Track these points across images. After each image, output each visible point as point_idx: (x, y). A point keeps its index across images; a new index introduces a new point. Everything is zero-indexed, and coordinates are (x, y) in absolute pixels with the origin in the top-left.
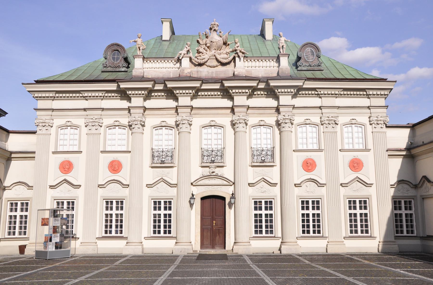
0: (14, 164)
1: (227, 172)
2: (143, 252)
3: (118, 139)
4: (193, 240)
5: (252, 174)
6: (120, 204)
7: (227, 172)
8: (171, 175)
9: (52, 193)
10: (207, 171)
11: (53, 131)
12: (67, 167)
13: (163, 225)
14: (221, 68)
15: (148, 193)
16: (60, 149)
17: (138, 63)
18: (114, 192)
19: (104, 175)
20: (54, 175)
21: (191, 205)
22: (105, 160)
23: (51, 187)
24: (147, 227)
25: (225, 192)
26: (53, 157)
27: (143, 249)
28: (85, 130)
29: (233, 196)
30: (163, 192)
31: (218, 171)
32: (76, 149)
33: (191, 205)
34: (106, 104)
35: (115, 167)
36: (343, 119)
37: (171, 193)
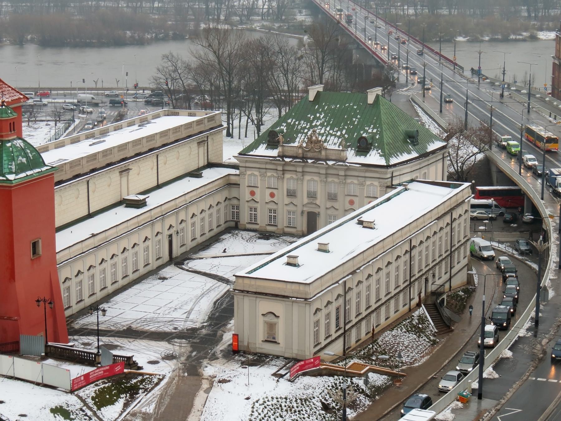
3: (273, 182)
6: (275, 211)
7: (318, 202)
8: (295, 201)
11: (246, 177)
12: (253, 193)
14: (315, 154)
19: (268, 199)
20: (248, 197)
21: (302, 215)
22: (268, 192)
23: (247, 201)
25: (316, 210)
28: (259, 178)
29: (319, 213)
33: (302, 215)
35: (272, 195)
36: (368, 183)
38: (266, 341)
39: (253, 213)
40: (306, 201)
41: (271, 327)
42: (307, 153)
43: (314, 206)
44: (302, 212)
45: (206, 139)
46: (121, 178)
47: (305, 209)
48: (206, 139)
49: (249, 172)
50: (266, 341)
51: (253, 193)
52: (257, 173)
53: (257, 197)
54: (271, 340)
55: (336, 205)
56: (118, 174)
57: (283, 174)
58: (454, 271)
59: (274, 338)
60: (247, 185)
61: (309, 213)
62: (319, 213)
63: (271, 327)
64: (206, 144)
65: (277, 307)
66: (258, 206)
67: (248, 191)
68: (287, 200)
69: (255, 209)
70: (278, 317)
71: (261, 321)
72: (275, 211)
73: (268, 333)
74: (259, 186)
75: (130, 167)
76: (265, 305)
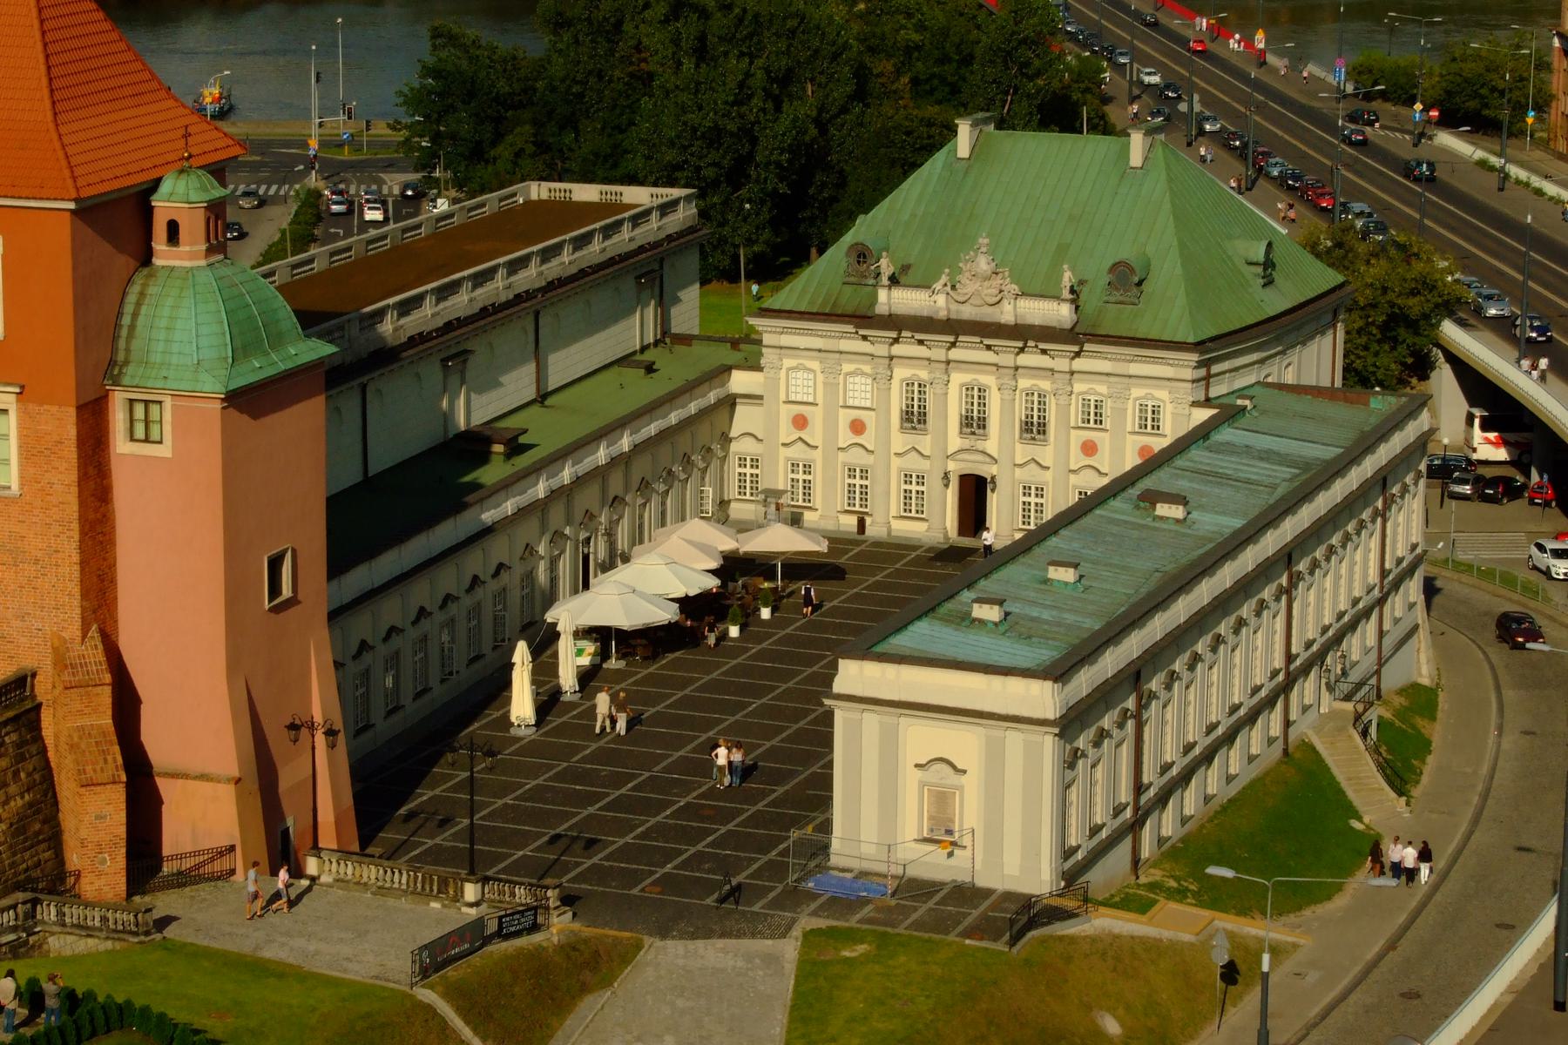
0: (740, 409)
1: (991, 446)
2: (889, 533)
3: (860, 390)
4: (948, 524)
5: (1022, 452)
6: (864, 473)
7: (991, 446)
8: (925, 443)
9: (784, 452)
10: (967, 443)
11: (783, 373)
12: (800, 422)
13: (912, 504)
15: (896, 462)
16: (793, 398)
17: (882, 295)
18: (858, 458)
19: (845, 437)
20: (786, 432)
21: (947, 486)
22: (845, 417)
24: (895, 507)
25: (986, 470)
26: (784, 408)
27: (889, 533)
28: (820, 378)
30: (915, 464)
31: (980, 445)
32: (811, 399)
34: (846, 345)
35: (858, 427)
37: (922, 465)
38: (926, 840)
39: (801, 477)
40: (955, 441)
41: (942, 801)
42: (963, 308)
43: (980, 457)
44: (946, 476)
45: (656, 267)
46: (445, 377)
47: (952, 466)
48: (656, 267)
49: (788, 362)
50: (926, 840)
51: (800, 422)
52: (815, 365)
53: (815, 434)
54: (943, 835)
55: (1046, 454)
56: (438, 366)
57: (890, 368)
58: (1388, 642)
59: (949, 832)
60: (783, 397)
61: (964, 478)
62: (993, 478)
63: (942, 801)
64: (657, 282)
65: (963, 742)
66: (817, 455)
67: (787, 413)
68: (899, 441)
69: (808, 469)
70: (965, 772)
71: (911, 780)
72: (864, 473)
73: (931, 818)
74: (820, 400)
75: (468, 346)
76: (923, 739)
